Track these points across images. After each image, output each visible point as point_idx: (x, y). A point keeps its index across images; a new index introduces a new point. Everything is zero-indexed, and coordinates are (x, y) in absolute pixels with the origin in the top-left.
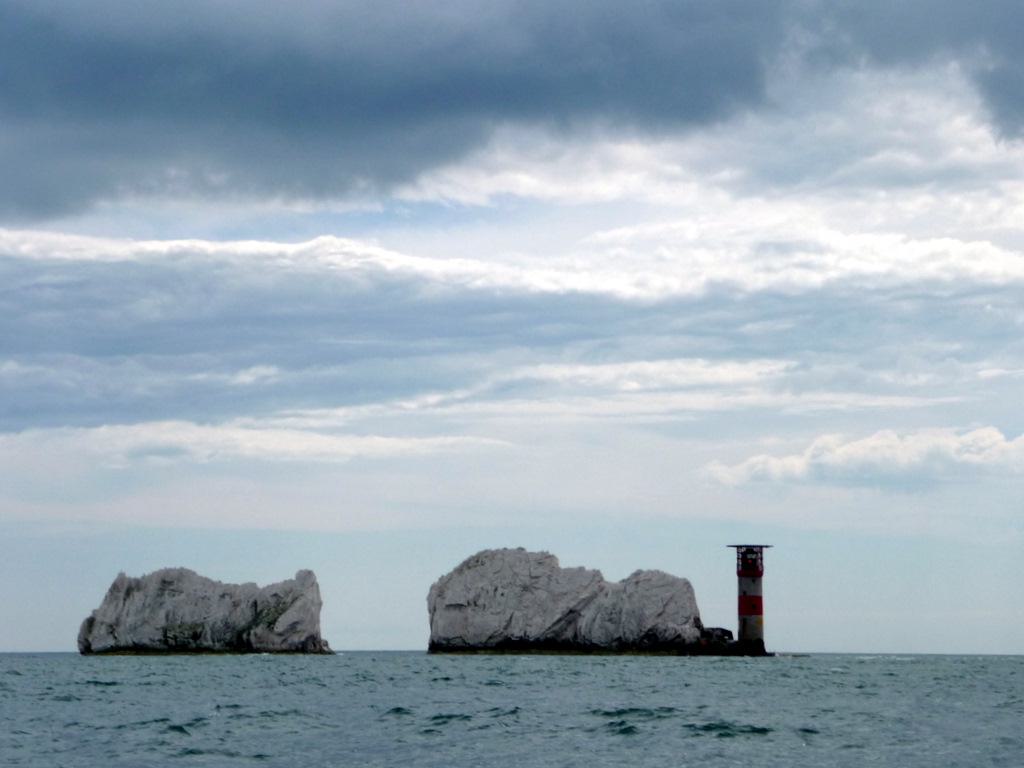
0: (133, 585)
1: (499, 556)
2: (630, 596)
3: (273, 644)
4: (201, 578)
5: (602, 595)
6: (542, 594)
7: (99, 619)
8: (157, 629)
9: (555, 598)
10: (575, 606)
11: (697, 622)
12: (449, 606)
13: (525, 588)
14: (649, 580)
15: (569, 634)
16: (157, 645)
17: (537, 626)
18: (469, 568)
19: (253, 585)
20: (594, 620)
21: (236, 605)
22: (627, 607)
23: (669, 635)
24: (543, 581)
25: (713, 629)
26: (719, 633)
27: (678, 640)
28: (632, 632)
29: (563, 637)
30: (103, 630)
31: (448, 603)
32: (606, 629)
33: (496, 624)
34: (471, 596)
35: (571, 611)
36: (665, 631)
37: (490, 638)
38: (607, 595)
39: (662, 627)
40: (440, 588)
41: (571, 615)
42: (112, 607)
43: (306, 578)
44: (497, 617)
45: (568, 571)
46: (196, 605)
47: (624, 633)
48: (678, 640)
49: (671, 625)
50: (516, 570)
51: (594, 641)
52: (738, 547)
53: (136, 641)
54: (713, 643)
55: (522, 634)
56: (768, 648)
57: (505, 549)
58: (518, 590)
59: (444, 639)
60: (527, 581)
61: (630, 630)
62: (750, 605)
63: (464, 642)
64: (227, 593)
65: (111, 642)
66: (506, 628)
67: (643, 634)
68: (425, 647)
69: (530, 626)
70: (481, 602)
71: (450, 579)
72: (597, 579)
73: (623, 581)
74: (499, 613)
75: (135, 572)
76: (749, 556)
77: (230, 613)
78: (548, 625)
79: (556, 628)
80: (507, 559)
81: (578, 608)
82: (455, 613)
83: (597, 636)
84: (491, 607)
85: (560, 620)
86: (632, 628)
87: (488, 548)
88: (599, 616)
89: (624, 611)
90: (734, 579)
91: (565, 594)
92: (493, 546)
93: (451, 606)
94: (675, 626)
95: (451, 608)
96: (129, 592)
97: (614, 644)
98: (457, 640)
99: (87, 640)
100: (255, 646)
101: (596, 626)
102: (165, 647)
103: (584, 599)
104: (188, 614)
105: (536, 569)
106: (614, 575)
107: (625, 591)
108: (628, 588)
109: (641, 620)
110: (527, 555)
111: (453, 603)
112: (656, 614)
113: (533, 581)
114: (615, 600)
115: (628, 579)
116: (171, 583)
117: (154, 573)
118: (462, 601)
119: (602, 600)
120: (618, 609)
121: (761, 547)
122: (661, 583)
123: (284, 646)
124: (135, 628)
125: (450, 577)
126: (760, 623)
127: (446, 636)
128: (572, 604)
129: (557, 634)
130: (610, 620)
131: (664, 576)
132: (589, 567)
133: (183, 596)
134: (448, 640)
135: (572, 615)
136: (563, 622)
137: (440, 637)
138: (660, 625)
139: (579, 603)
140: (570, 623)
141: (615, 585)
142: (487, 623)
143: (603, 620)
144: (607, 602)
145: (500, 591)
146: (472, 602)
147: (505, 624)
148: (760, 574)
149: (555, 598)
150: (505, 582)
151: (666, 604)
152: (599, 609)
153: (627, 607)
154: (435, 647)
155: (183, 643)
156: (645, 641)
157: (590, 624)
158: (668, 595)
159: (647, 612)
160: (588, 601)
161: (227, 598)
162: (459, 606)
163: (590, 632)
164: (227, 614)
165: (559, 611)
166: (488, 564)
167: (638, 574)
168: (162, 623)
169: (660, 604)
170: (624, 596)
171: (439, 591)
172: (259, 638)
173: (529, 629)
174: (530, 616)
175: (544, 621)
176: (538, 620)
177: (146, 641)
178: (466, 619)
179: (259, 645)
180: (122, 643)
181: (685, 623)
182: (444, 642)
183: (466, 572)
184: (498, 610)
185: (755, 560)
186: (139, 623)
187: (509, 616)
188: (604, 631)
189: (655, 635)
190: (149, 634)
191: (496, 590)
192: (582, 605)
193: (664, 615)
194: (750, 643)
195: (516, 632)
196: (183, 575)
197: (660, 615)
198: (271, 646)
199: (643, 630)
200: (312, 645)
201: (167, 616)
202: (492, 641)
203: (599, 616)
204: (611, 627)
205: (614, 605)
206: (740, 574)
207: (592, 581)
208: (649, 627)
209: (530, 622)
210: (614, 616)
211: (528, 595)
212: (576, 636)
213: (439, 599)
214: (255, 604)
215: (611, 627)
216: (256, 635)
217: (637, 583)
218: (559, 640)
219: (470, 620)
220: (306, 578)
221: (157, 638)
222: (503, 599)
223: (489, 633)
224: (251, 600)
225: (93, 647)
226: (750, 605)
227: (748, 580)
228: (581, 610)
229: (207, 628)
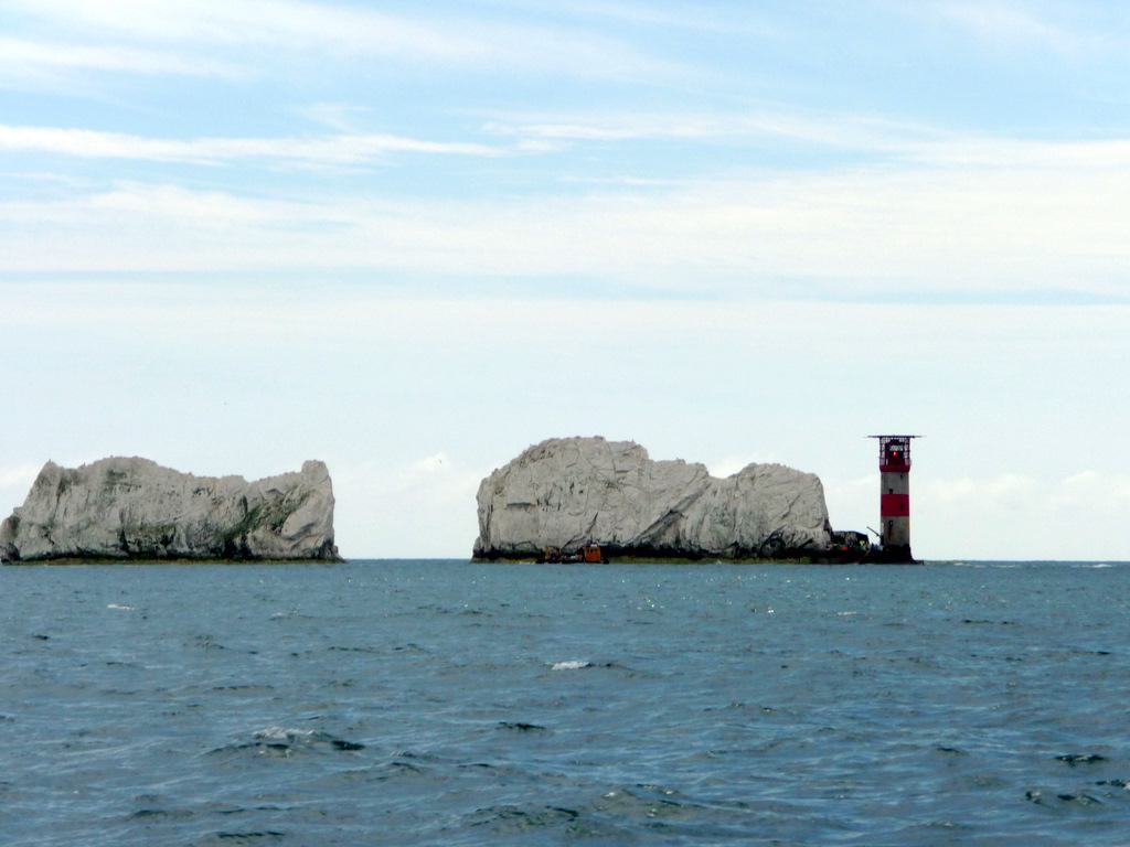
0: (69, 477)
1: (572, 446)
2: (745, 495)
3: (281, 550)
4: (163, 469)
5: (709, 492)
6: (632, 492)
7: (26, 518)
8: (110, 532)
9: (650, 497)
10: (676, 507)
11: (827, 528)
12: (512, 506)
13: (610, 485)
14: (769, 475)
15: (668, 539)
16: (111, 551)
17: (627, 534)
18: (534, 460)
19: (240, 478)
20: (701, 523)
21: (217, 502)
22: (741, 507)
23: (799, 540)
24: (632, 475)
25: (845, 533)
26: (853, 537)
27: (808, 545)
28: (752, 537)
29: (661, 543)
30: (34, 533)
31: (510, 502)
32: (718, 533)
33: (577, 526)
34: (541, 493)
35: (671, 512)
36: (794, 535)
37: (569, 543)
38: (715, 493)
39: (788, 531)
40: (497, 483)
41: (671, 517)
42: (43, 504)
43: (316, 470)
44: (578, 518)
45: (664, 464)
46: (161, 502)
47: (742, 537)
48: (808, 545)
49: (800, 528)
50: (597, 463)
51: (703, 547)
52: (881, 437)
53: (83, 547)
54: (847, 550)
55: (610, 538)
56: (916, 555)
57: (578, 438)
58: (600, 486)
59: (509, 545)
60: (612, 477)
61: (749, 535)
62: (895, 505)
63: (536, 548)
64: (201, 488)
65: (46, 548)
66: (588, 532)
67: (766, 538)
68: (469, 555)
69: (621, 529)
70: (554, 501)
72: (702, 474)
73: (734, 476)
74: (578, 514)
75: (70, 462)
76: (895, 448)
77: (210, 513)
78: (642, 529)
79: (652, 532)
80: (581, 450)
81: (680, 508)
82: (520, 514)
83: (706, 540)
84: (568, 506)
85: (658, 522)
86: (752, 532)
87: (555, 436)
88: (707, 518)
89: (739, 510)
90: (878, 475)
91: (664, 491)
92: (562, 435)
93: (515, 504)
94: (805, 529)
95: (515, 508)
96: (62, 487)
97: (729, 550)
98: (525, 545)
99: (11, 545)
100: (254, 552)
101: (705, 528)
102: (124, 553)
103: (687, 498)
104: (150, 514)
105: (620, 462)
106: (723, 469)
107: (737, 488)
108: (740, 485)
109: (762, 523)
110: (609, 445)
111: (517, 501)
112: (781, 515)
113: (618, 476)
114: (726, 499)
115: (739, 475)
116: (122, 475)
117: (96, 463)
118: (530, 499)
119: (708, 498)
120: (730, 509)
121: (908, 438)
122: (786, 479)
123: (295, 553)
124: (79, 531)
125: (508, 470)
126: (907, 525)
127: (510, 541)
128: (673, 504)
129: (654, 539)
130: (722, 522)
131: (787, 471)
132: (690, 460)
133: (141, 491)
134: (514, 546)
135: (673, 515)
136: (661, 525)
137: (502, 543)
138: (785, 528)
139: (680, 503)
140: (669, 525)
141: (724, 481)
142: (562, 526)
143: (713, 522)
144: (716, 501)
145: (577, 488)
146: (542, 501)
147: (588, 527)
148: (906, 469)
149: (650, 497)
150: (582, 477)
151: (793, 504)
152: (706, 509)
153: (741, 507)
154: (487, 554)
155: (146, 549)
156: (769, 546)
157: (696, 527)
158: (795, 493)
159: (770, 514)
160: (692, 500)
161: (204, 494)
162: (526, 505)
163: (697, 536)
164: (206, 514)
165: (656, 511)
166: (558, 455)
167: (751, 468)
168: (116, 523)
169: (786, 505)
170: (737, 494)
171: (495, 487)
172: (261, 543)
173: (619, 533)
174: (619, 518)
175: (638, 524)
176: (630, 522)
177: (95, 547)
178: (535, 520)
179: (260, 552)
180: (63, 549)
181: (817, 526)
182: (508, 548)
183: (531, 465)
184: (578, 511)
185: (901, 454)
186: (84, 524)
188: (715, 535)
189: (779, 540)
190: (101, 537)
191: (572, 486)
192: (685, 504)
193: (790, 517)
194: (895, 550)
195: (603, 536)
196: (137, 464)
197: (785, 516)
198: (278, 553)
199: (766, 533)
200: (326, 554)
201: (122, 516)
202: (571, 546)
203: (707, 518)
204: (724, 530)
205: (726, 506)
206: (883, 469)
207: (696, 476)
208: (773, 530)
209: (618, 524)
210: (726, 517)
211: (614, 494)
212: (678, 541)
213: (496, 498)
214: (244, 501)
215: (724, 530)
216: (255, 539)
217: (752, 479)
218: (656, 545)
219: (542, 522)
220: (316, 470)
221: (110, 543)
222: (584, 497)
223: (569, 538)
224: (238, 497)
225: (22, 555)
226: (895, 505)
227: (891, 476)
228: (684, 510)
229: (181, 531)
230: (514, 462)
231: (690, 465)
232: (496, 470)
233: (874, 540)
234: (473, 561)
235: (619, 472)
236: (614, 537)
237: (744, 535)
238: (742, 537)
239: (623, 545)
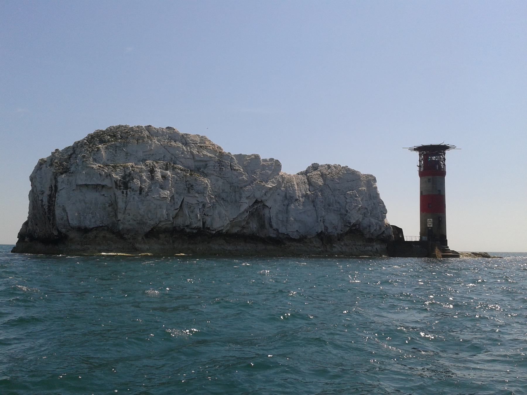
28: (335, 228)
31: (80, 183)
35: (257, 202)
36: (370, 226)
39: (366, 222)
55: (200, 224)
62: (433, 204)
68: (14, 240)
71: (70, 156)
73: (302, 173)
82: (92, 196)
132: (264, 156)
138: (360, 220)
148: (443, 173)
173: (208, 220)
178: (113, 204)
185: (438, 163)
187: (180, 203)
194: (434, 241)
208: (353, 221)
226: (433, 204)
230: (78, 146)
231: (265, 160)
232: (57, 150)
233: (412, 232)
234: (15, 250)
235: (197, 161)
236: (204, 223)
237: (328, 225)
238: (326, 228)
239: (214, 232)
